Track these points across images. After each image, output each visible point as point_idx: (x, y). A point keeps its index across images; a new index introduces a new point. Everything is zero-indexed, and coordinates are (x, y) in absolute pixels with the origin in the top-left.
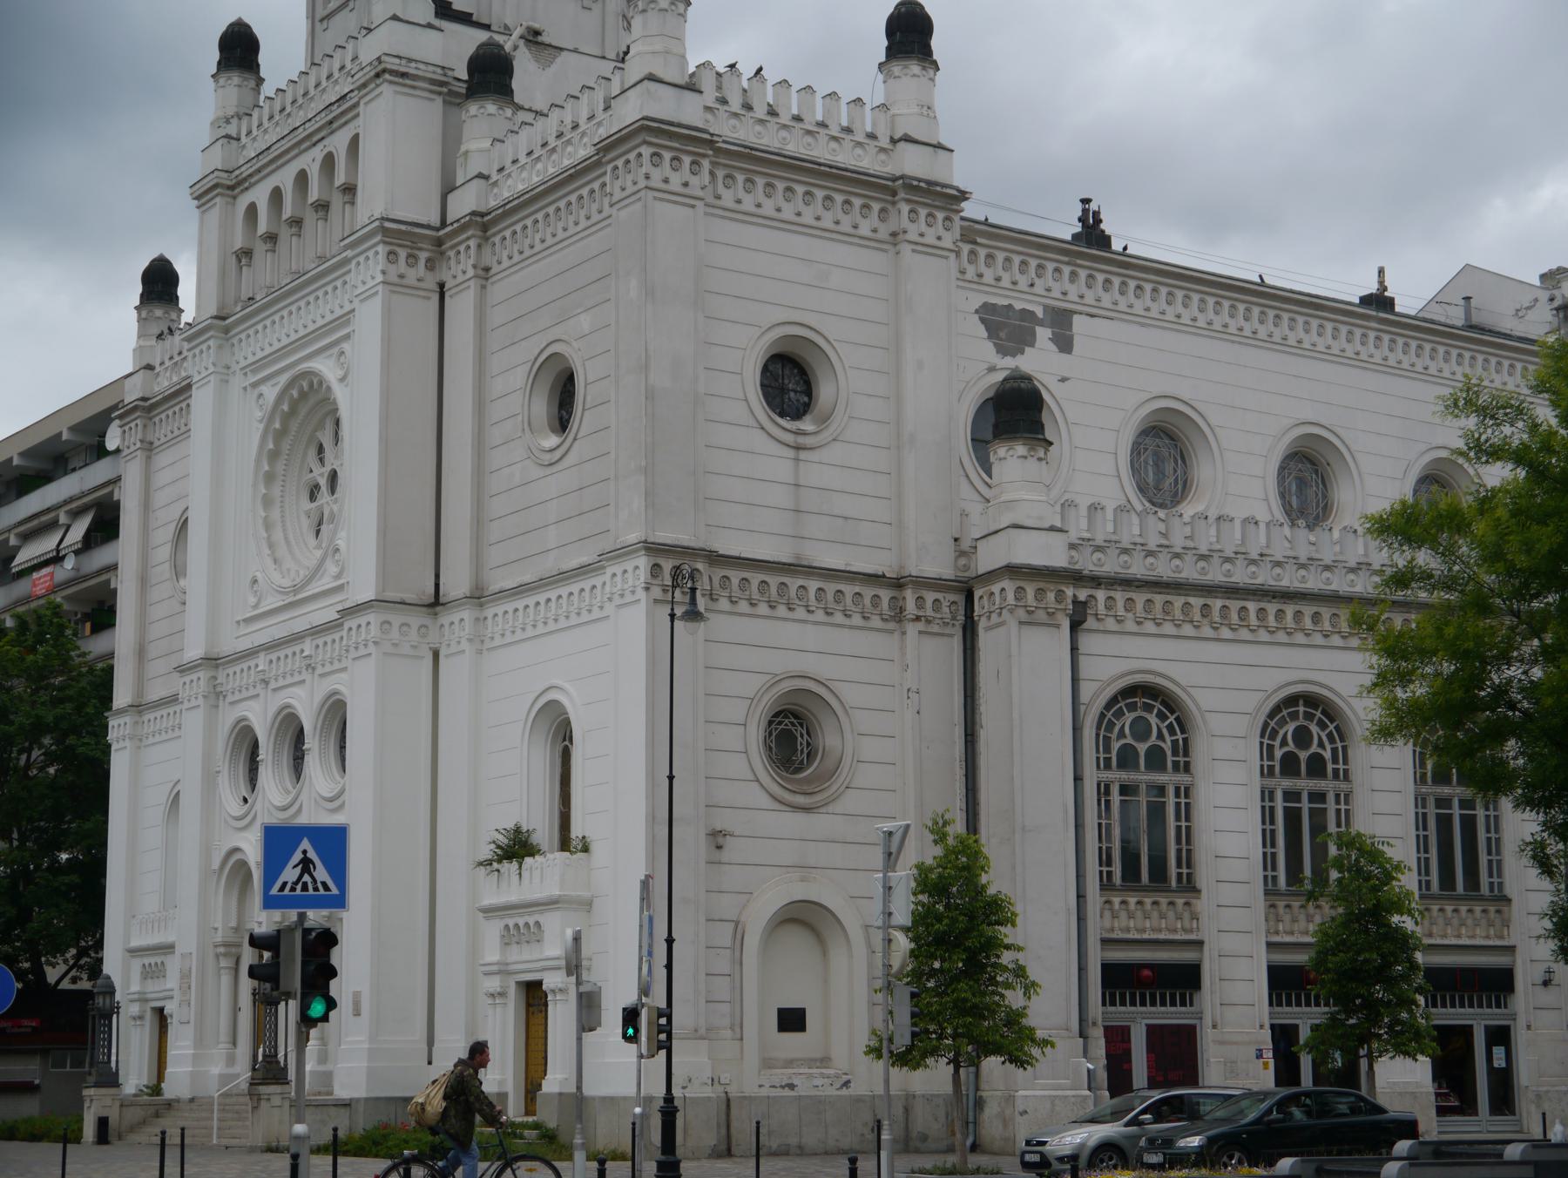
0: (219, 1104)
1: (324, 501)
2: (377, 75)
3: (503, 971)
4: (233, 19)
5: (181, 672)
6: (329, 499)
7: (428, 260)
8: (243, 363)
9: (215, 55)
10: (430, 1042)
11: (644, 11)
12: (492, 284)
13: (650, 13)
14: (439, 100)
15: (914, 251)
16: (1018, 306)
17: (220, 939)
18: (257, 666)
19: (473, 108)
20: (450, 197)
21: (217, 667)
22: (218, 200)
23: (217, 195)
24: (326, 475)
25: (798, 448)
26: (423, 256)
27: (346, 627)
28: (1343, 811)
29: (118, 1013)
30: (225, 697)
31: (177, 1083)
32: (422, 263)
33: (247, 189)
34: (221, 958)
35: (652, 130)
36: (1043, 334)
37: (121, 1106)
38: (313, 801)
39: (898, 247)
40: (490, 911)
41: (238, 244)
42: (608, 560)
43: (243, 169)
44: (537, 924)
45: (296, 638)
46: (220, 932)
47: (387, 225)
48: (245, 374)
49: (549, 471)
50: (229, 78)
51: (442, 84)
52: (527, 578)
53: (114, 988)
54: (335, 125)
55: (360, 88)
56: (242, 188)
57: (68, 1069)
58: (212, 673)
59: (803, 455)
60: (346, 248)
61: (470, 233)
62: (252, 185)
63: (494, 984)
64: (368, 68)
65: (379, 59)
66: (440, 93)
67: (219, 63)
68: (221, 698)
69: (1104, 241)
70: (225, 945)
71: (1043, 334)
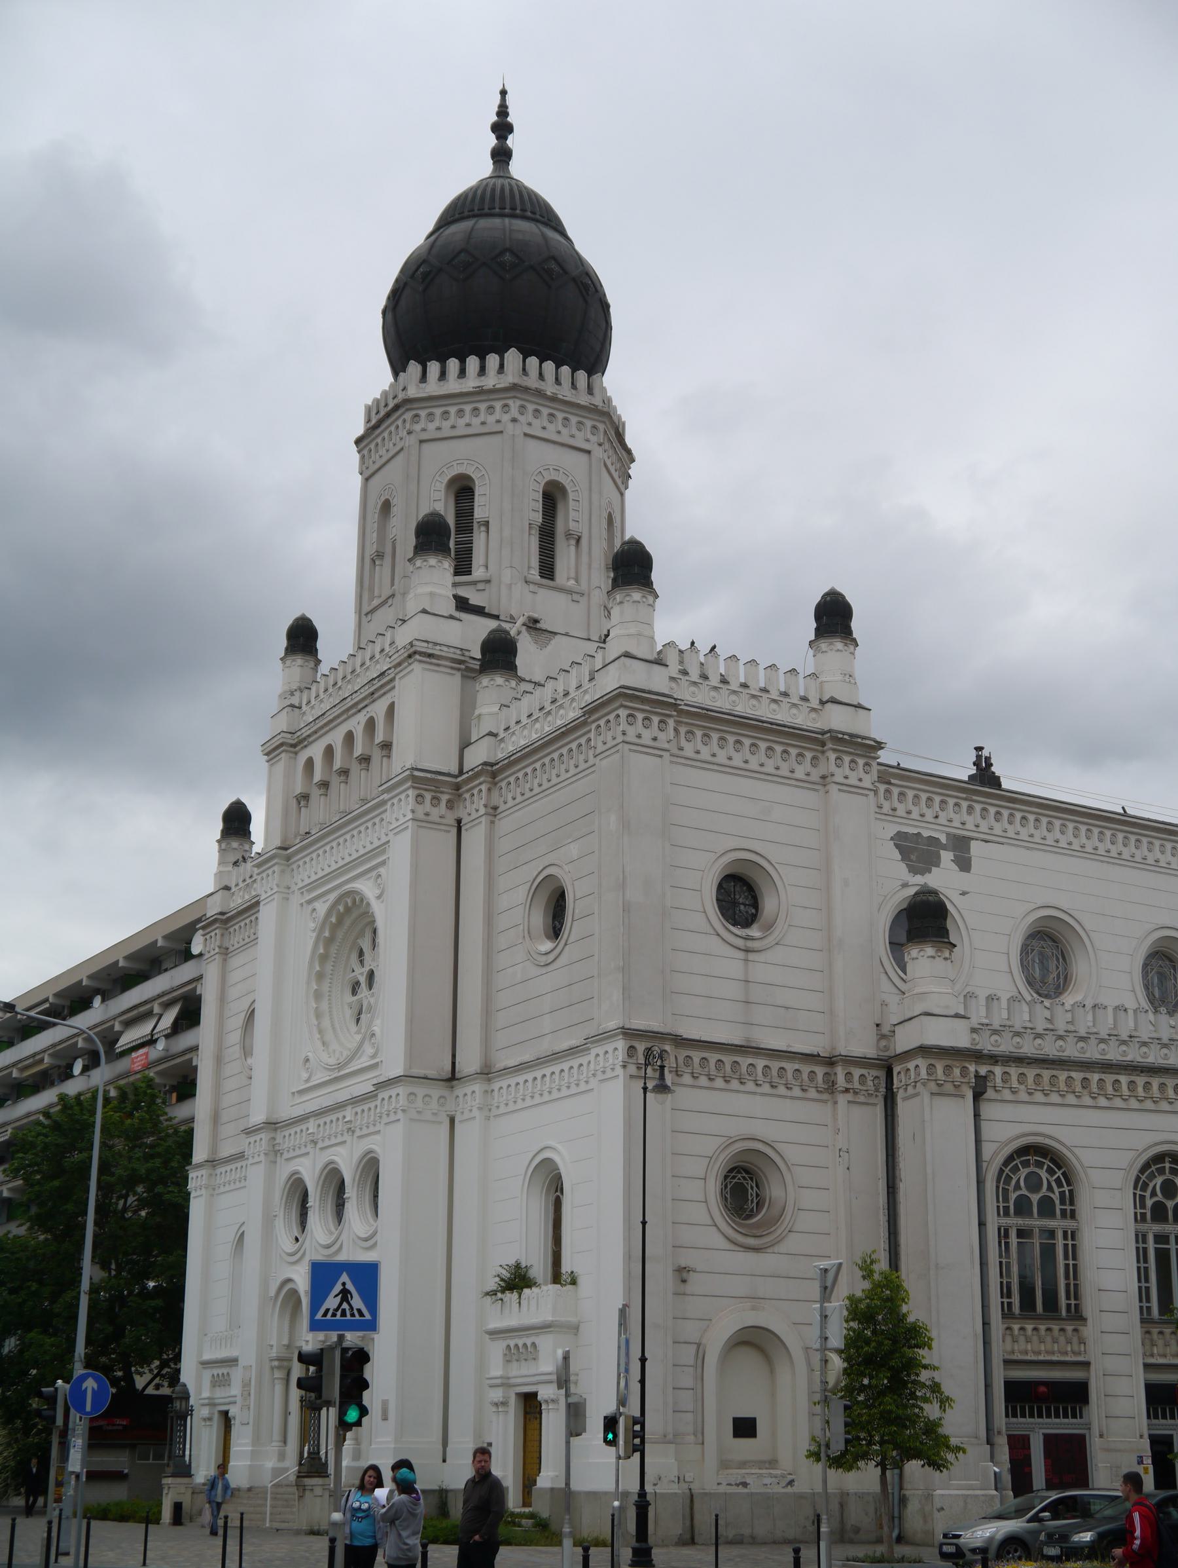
0: (271, 1493)
1: (362, 995)
2: (410, 656)
3: (505, 1384)
4: (297, 615)
5: (247, 1133)
7: (449, 801)
8: (301, 885)
9: (283, 642)
10: (445, 1443)
11: (621, 603)
12: (499, 820)
13: (626, 604)
14: (458, 674)
15: (839, 790)
16: (926, 834)
17: (275, 1355)
18: (308, 1129)
19: (485, 681)
20: (466, 751)
21: (276, 1129)
22: (283, 755)
23: (283, 751)
24: (365, 974)
25: (747, 951)
26: (444, 798)
27: (380, 1096)
29: (191, 1415)
30: (282, 1154)
31: (238, 1474)
33: (306, 746)
34: (275, 1370)
35: (627, 696)
36: (947, 856)
37: (193, 1493)
39: (827, 788)
40: (495, 1334)
41: (299, 789)
42: (592, 1043)
43: (303, 731)
44: (534, 1344)
45: (340, 1106)
46: (274, 1350)
47: (416, 773)
48: (302, 893)
49: (544, 970)
50: (294, 660)
52: (527, 1057)
53: (188, 1394)
54: (376, 696)
55: (395, 667)
56: (302, 745)
58: (272, 1135)
59: (751, 956)
60: (383, 792)
61: (482, 779)
63: (497, 1395)
64: (403, 651)
65: (411, 644)
66: (459, 669)
67: (287, 649)
68: (279, 1155)
69: (995, 782)
70: (279, 1359)
71: (947, 856)
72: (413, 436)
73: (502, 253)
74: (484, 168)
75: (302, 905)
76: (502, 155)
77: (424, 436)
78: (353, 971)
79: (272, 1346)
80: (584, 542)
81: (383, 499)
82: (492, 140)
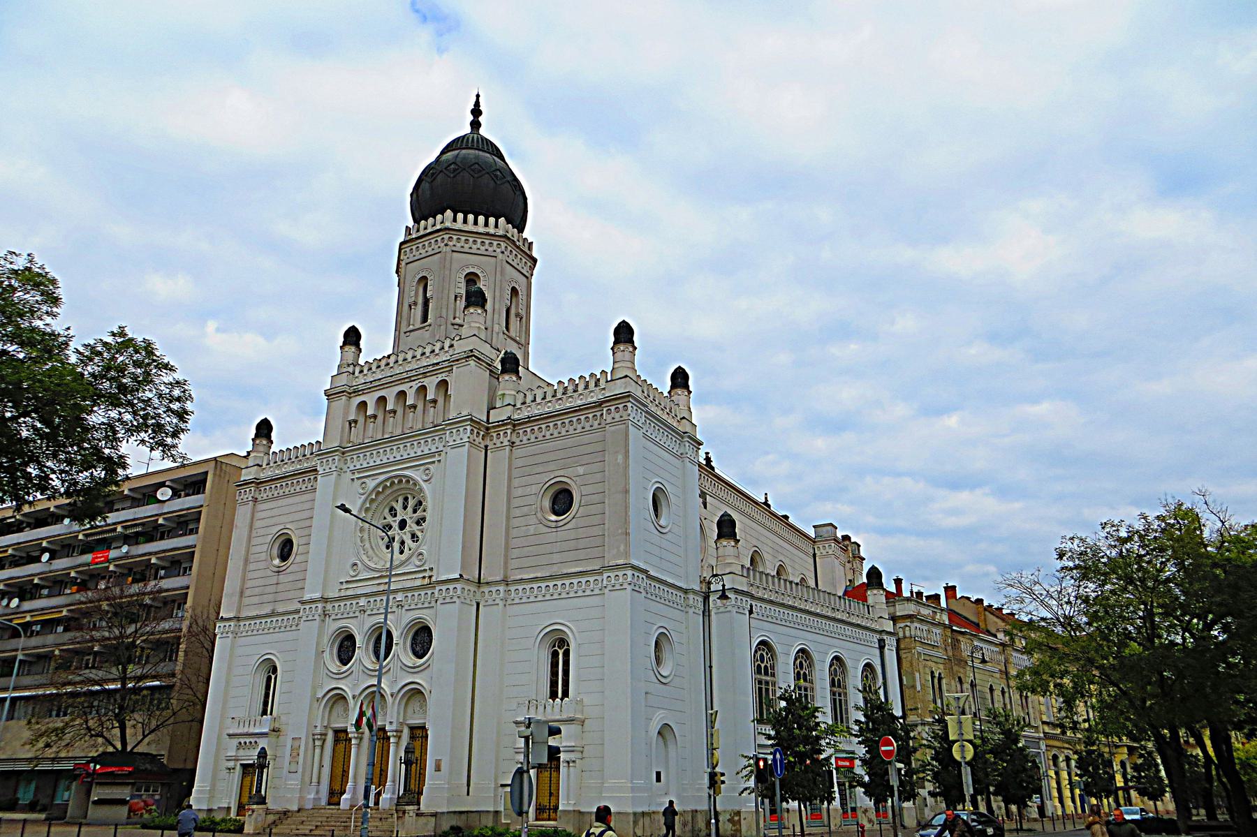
2: (468, 357)
8: (352, 468)
10: (468, 785)
21: (326, 602)
22: (344, 397)
26: (482, 433)
27: (438, 588)
28: (764, 690)
32: (481, 436)
41: (352, 417)
49: (555, 530)
51: (490, 365)
52: (539, 575)
58: (324, 605)
62: (363, 393)
65: (471, 351)
72: (448, 248)
74: (467, 130)
76: (476, 125)
77: (454, 249)
78: (385, 518)
79: (316, 727)
80: (524, 319)
81: (420, 275)
82: (471, 118)
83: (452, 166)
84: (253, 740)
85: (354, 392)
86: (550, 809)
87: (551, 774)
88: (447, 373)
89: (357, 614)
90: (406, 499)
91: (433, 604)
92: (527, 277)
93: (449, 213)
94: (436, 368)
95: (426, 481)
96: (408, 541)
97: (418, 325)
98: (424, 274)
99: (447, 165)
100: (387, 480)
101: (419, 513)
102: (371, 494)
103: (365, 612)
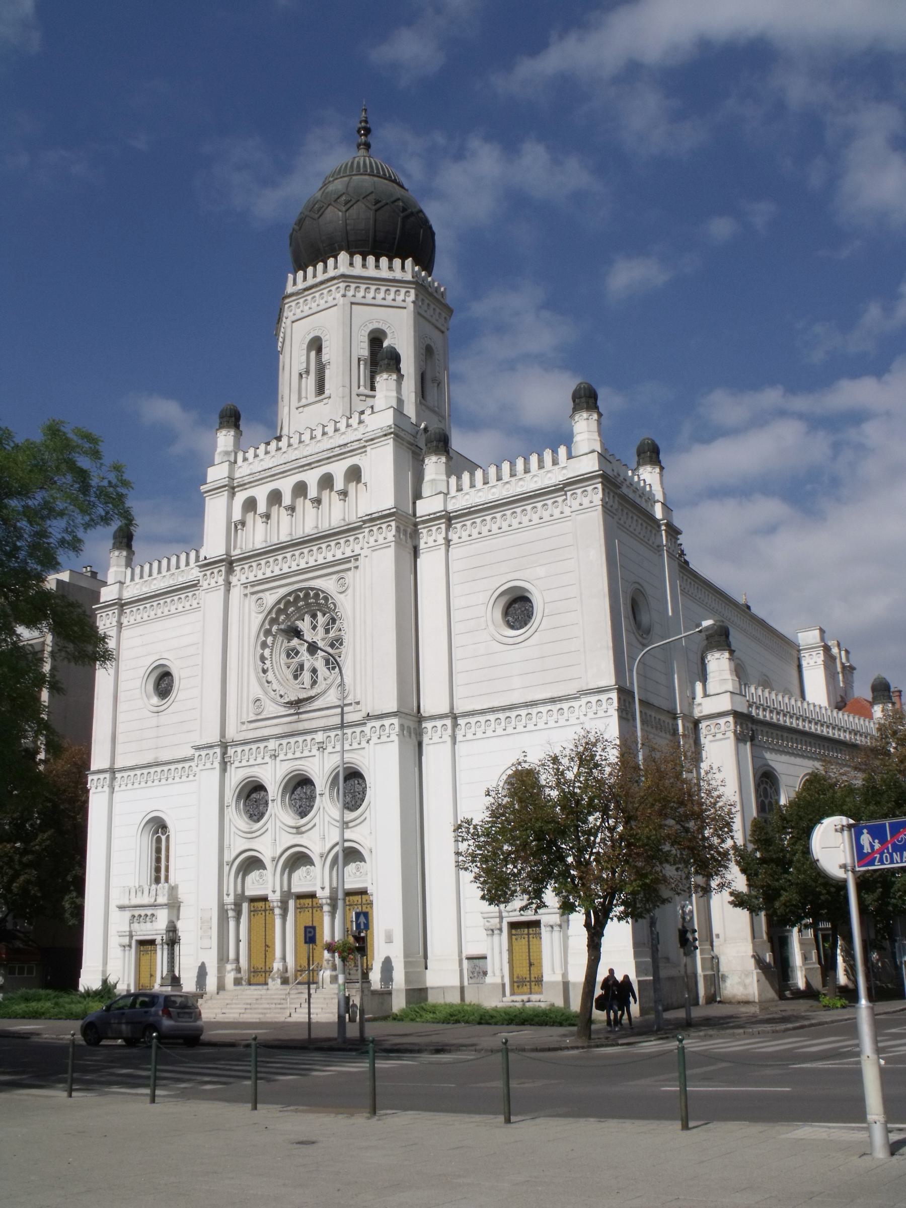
5: (196, 749)
6: (309, 657)
8: (244, 581)
13: (590, 420)
14: (410, 453)
20: (418, 502)
38: (326, 823)
57: (17, 975)
64: (379, 431)
73: (395, 201)
75: (246, 595)
83: (343, 198)
84: (149, 912)
85: (238, 486)
86: (530, 982)
87: (529, 941)
88: (358, 456)
89: (267, 759)
90: (314, 616)
91: (364, 744)
92: (443, 332)
93: (343, 256)
94: (344, 451)
95: (341, 593)
96: (322, 670)
97: (312, 397)
98: (316, 333)
99: (336, 196)
100: (290, 594)
101: (332, 634)
102: (270, 612)
103: (276, 757)
